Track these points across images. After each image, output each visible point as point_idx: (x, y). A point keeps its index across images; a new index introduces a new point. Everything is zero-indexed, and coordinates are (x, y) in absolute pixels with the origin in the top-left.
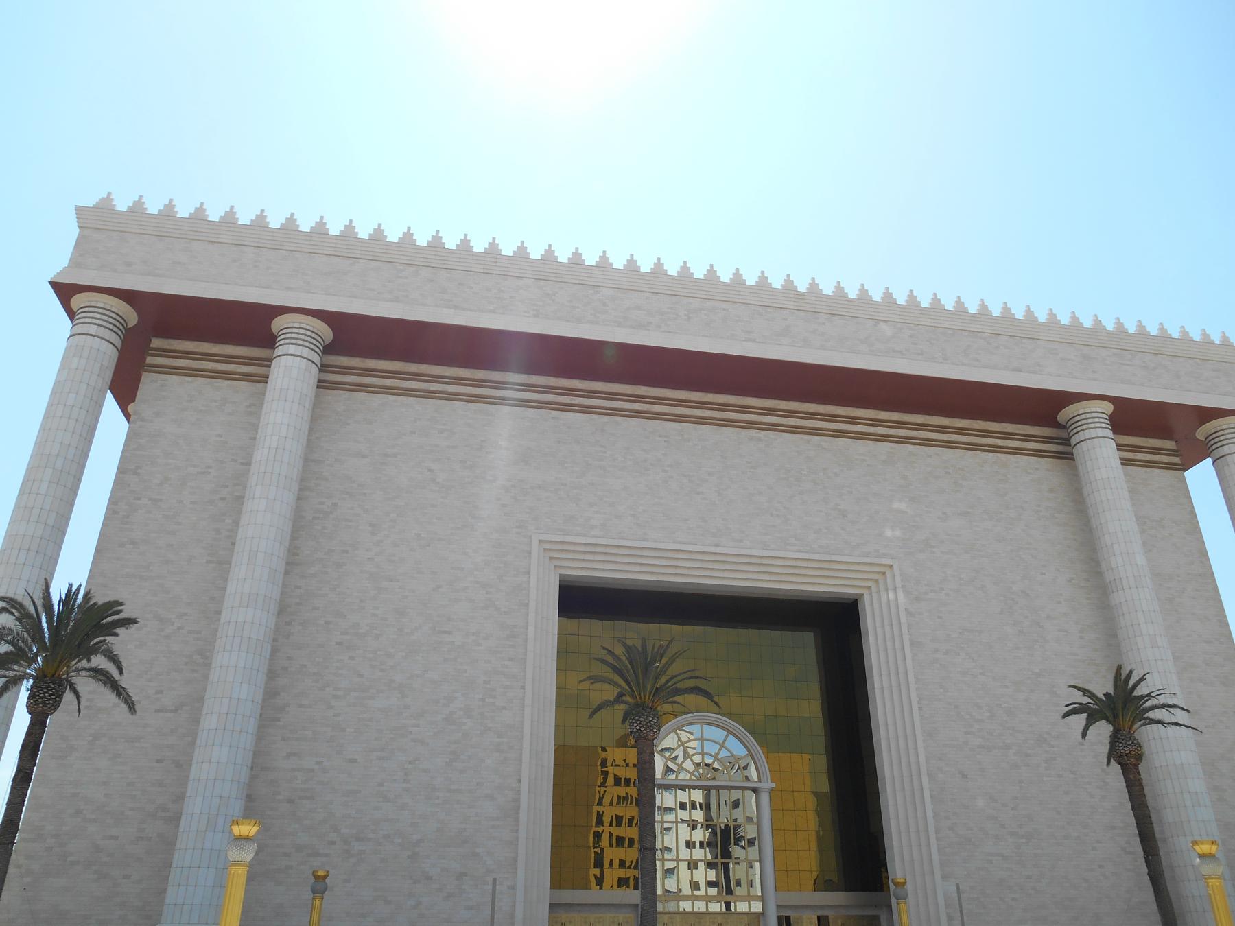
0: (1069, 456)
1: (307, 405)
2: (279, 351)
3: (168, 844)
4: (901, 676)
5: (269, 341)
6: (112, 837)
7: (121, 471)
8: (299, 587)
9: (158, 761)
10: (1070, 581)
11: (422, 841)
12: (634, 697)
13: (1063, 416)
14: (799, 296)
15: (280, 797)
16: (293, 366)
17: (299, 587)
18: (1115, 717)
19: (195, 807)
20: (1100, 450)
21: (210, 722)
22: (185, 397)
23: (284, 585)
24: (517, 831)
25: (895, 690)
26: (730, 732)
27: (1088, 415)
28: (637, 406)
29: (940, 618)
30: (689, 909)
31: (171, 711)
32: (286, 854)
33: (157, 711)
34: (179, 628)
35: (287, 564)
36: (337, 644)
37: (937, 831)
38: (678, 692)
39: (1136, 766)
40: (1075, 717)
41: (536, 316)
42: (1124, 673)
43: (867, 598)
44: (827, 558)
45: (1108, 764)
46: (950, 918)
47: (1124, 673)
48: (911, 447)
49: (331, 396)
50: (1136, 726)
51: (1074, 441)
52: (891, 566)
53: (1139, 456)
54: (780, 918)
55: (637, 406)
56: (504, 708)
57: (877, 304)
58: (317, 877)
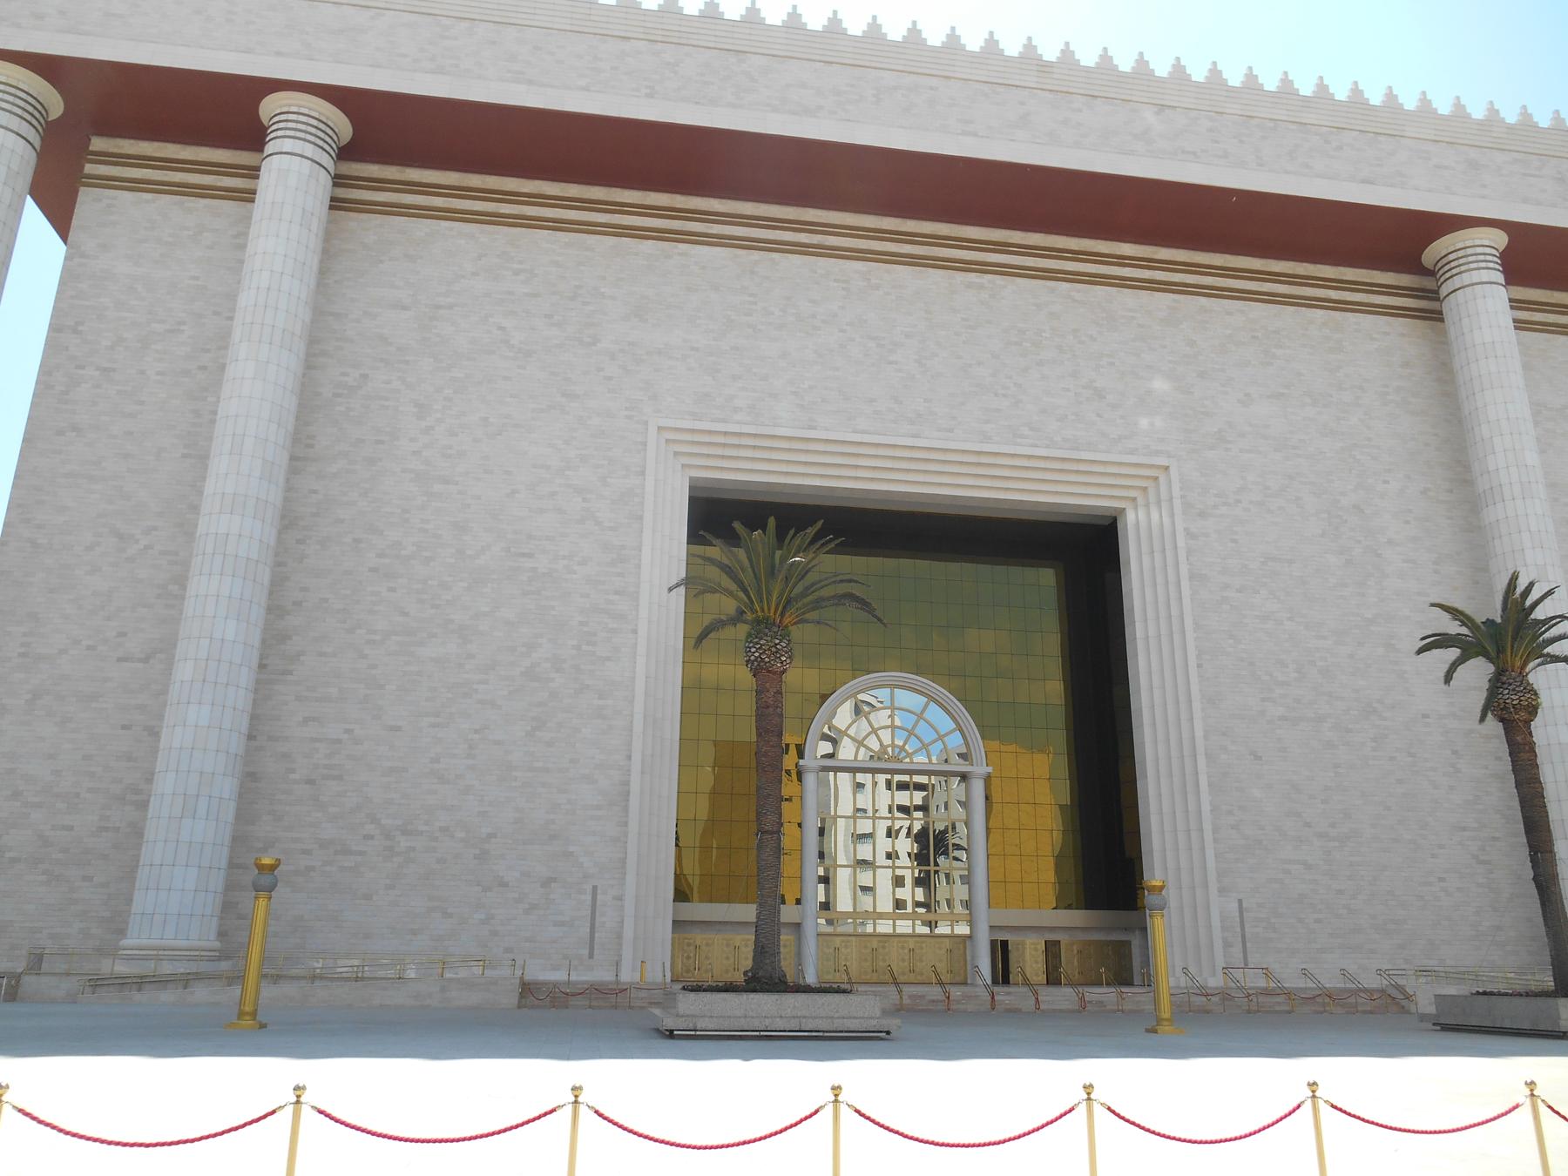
0: (1436, 316)
1: (314, 227)
2: (269, 149)
3: (137, 832)
4: (1175, 621)
5: (254, 137)
6: (64, 828)
7: (55, 328)
8: (315, 492)
9: (124, 727)
10: (1424, 492)
11: (491, 836)
12: (753, 611)
13: (1430, 256)
14: (1044, 67)
15: (292, 776)
16: (293, 172)
17: (315, 492)
18: (1500, 651)
19: (165, 784)
20: (1483, 302)
21: (184, 671)
22: (144, 222)
23: (289, 488)
24: (626, 824)
25: (1165, 640)
26: (931, 699)
27: (1469, 251)
28: (803, 238)
29: (1234, 541)
30: (869, 929)
31: (140, 660)
32: (305, 852)
33: (119, 660)
34: (146, 547)
35: (293, 458)
36: (372, 570)
37: (1215, 830)
38: (817, 605)
39: (1528, 723)
40: (1435, 651)
41: (650, 96)
42: (1522, 585)
43: (1130, 517)
44: (1075, 455)
45: (1482, 719)
46: (1227, 945)
47: (1522, 585)
48: (1203, 300)
49: (353, 221)
50: (1531, 665)
51: (1444, 291)
52: (1167, 468)
53: (1538, 317)
54: (993, 943)
55: (803, 238)
56: (608, 659)
57: (1160, 80)
58: (261, 868)
